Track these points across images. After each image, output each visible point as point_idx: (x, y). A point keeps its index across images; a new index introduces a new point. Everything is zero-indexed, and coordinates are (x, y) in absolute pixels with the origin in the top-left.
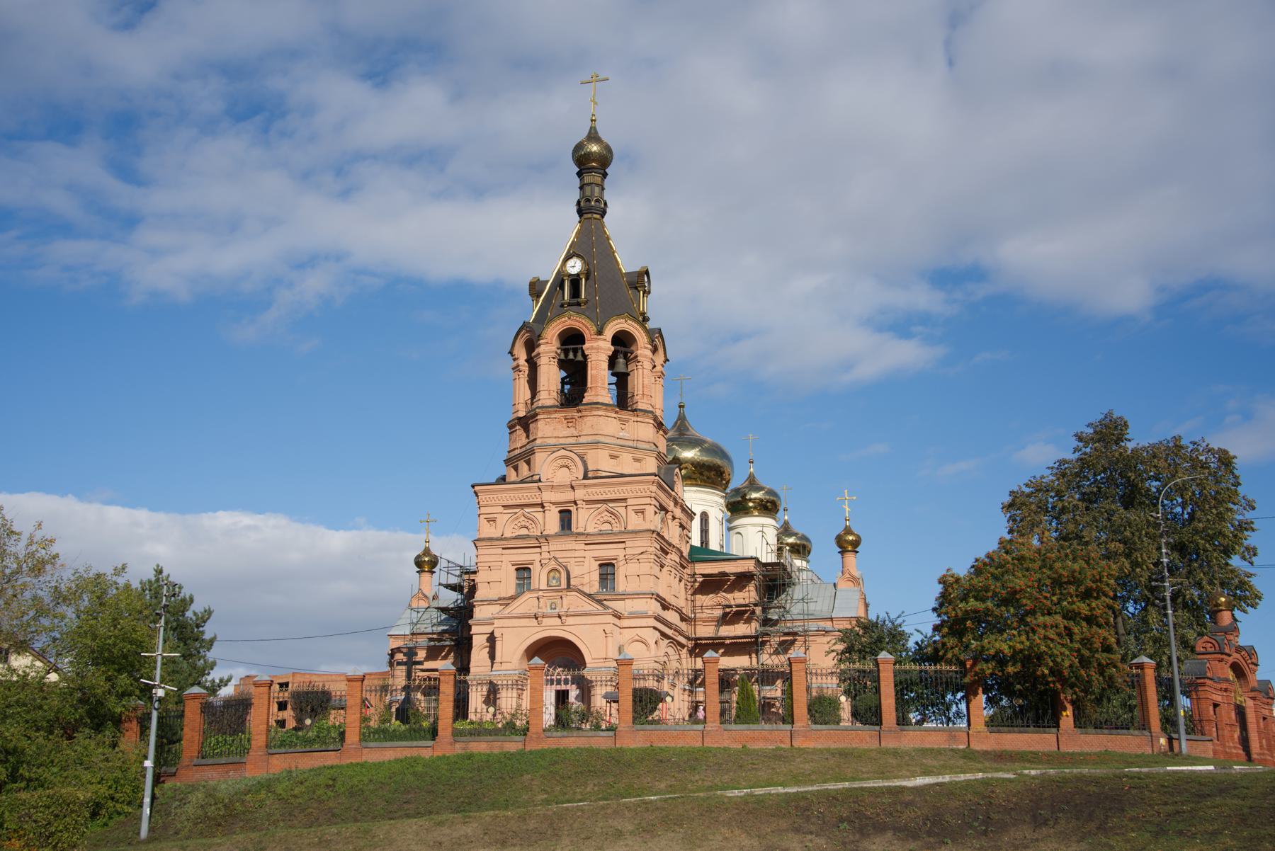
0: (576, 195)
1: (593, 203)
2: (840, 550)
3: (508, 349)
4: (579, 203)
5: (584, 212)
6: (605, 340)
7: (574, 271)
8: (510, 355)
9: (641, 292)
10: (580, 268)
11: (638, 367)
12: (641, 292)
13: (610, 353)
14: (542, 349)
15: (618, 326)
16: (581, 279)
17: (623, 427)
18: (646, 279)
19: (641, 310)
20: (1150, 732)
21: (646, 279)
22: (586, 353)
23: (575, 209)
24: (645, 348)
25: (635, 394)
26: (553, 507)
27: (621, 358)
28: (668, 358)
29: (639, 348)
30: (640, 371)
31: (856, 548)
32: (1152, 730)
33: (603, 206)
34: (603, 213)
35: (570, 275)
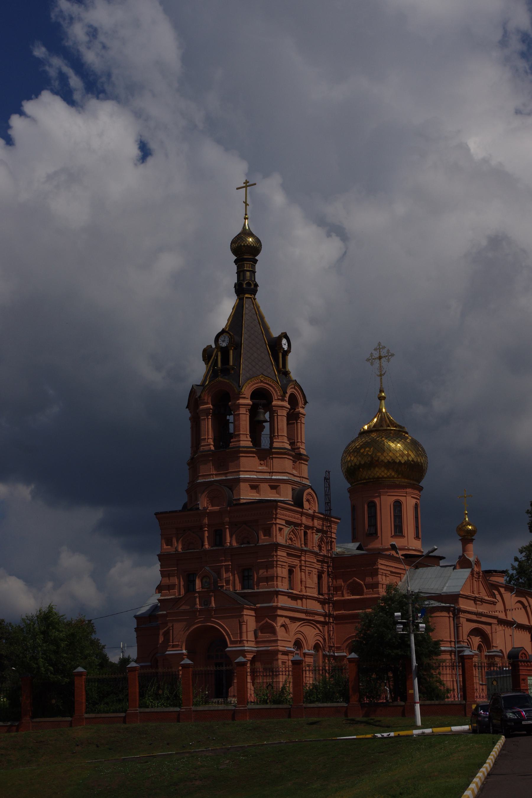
0: (234, 279)
1: (244, 286)
2: (461, 538)
6: (244, 398)
7: (224, 345)
8: (187, 409)
9: (281, 355)
12: (281, 355)
17: (262, 462)
18: (284, 341)
19: (281, 366)
20: (466, 702)
21: (284, 341)
24: (278, 399)
27: (260, 409)
28: (308, 401)
31: (473, 536)
32: (468, 700)
33: (252, 287)
34: (254, 291)
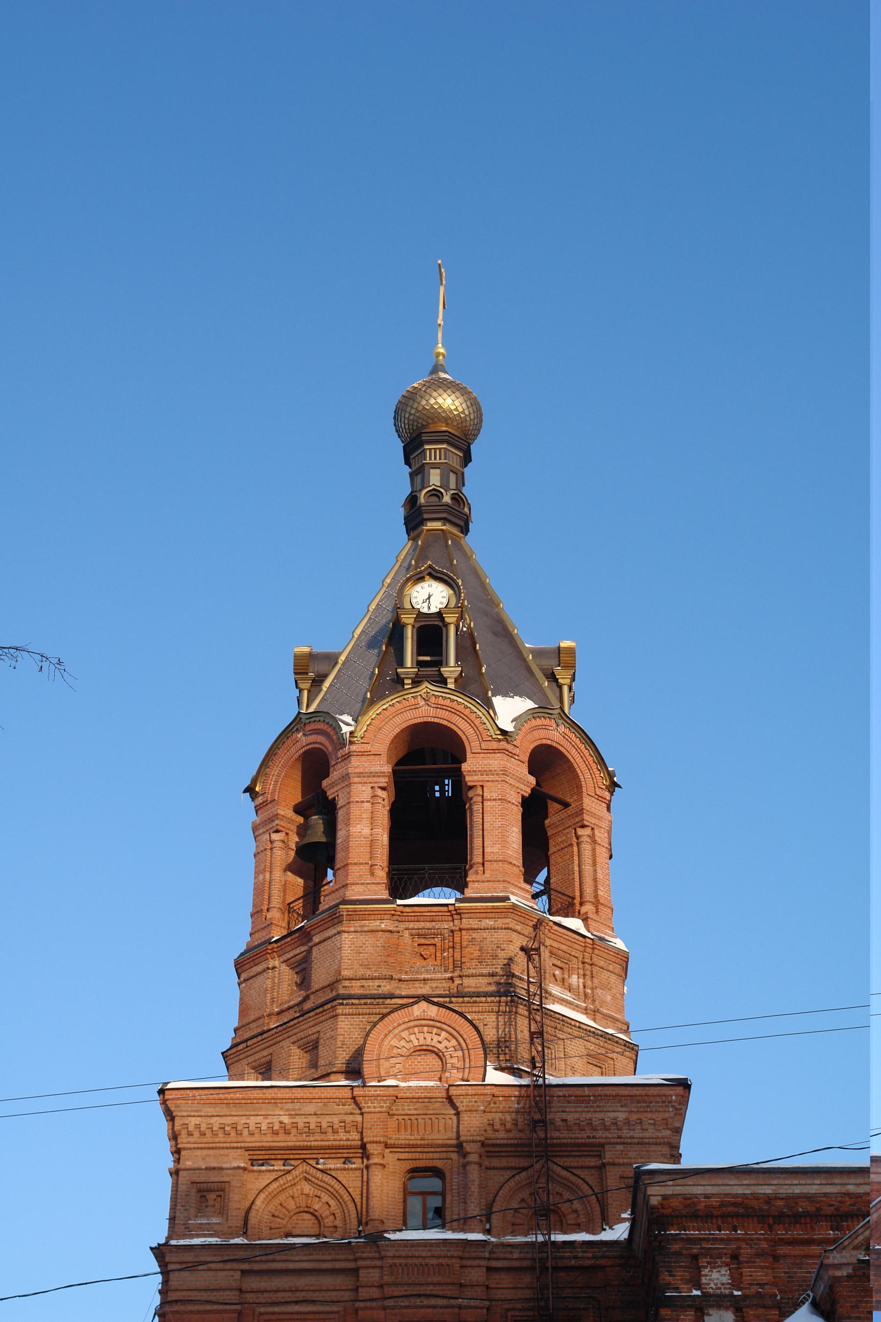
3: (248, 783)
4: (412, 501)
5: (426, 516)
10: (445, 601)
11: (582, 839)
13: (527, 792)
14: (356, 765)
15: (542, 733)
16: (446, 625)
22: (469, 779)
23: (401, 513)
25: (577, 901)
26: (390, 1158)
29: (585, 795)
30: (587, 848)
33: (466, 510)
35: (420, 615)
